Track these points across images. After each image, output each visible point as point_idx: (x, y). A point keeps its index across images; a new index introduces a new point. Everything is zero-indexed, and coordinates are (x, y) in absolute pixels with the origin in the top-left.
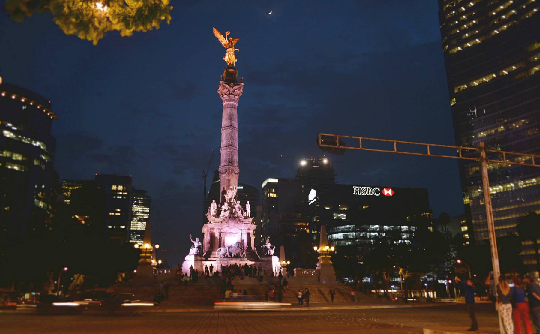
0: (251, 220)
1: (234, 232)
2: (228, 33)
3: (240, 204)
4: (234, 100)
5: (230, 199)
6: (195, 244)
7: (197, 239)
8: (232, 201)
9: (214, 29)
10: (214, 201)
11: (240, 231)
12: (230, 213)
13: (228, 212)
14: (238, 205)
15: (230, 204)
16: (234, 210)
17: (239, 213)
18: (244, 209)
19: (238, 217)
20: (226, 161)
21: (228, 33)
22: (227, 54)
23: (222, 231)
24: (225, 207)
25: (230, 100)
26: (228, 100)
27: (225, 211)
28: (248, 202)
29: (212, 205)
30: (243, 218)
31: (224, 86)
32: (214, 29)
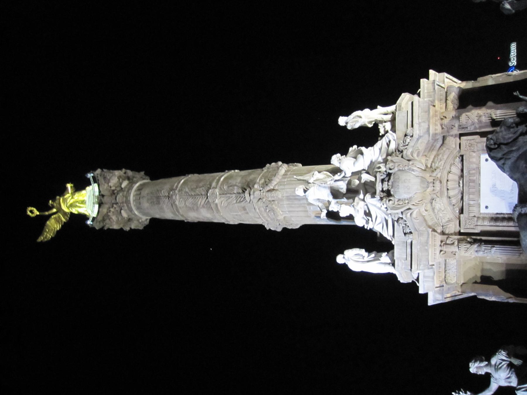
0: (405, 98)
1: (456, 170)
2: (33, 212)
3: (344, 152)
4: (128, 191)
5: (336, 194)
6: (504, 384)
7: (476, 368)
8: (343, 186)
9: (41, 239)
10: (340, 259)
11: (452, 142)
12: (369, 188)
13: (374, 204)
14: (350, 164)
15: (352, 193)
16: (366, 177)
17: (372, 154)
18: (369, 136)
19: (388, 155)
20: (244, 209)
21: (33, 212)
22: (75, 211)
23: (453, 228)
24: (358, 212)
25: (128, 202)
26: (128, 206)
27: (368, 214)
28: (342, 121)
29: (355, 267)
30: (391, 136)
31: (104, 220)
32: (41, 239)
